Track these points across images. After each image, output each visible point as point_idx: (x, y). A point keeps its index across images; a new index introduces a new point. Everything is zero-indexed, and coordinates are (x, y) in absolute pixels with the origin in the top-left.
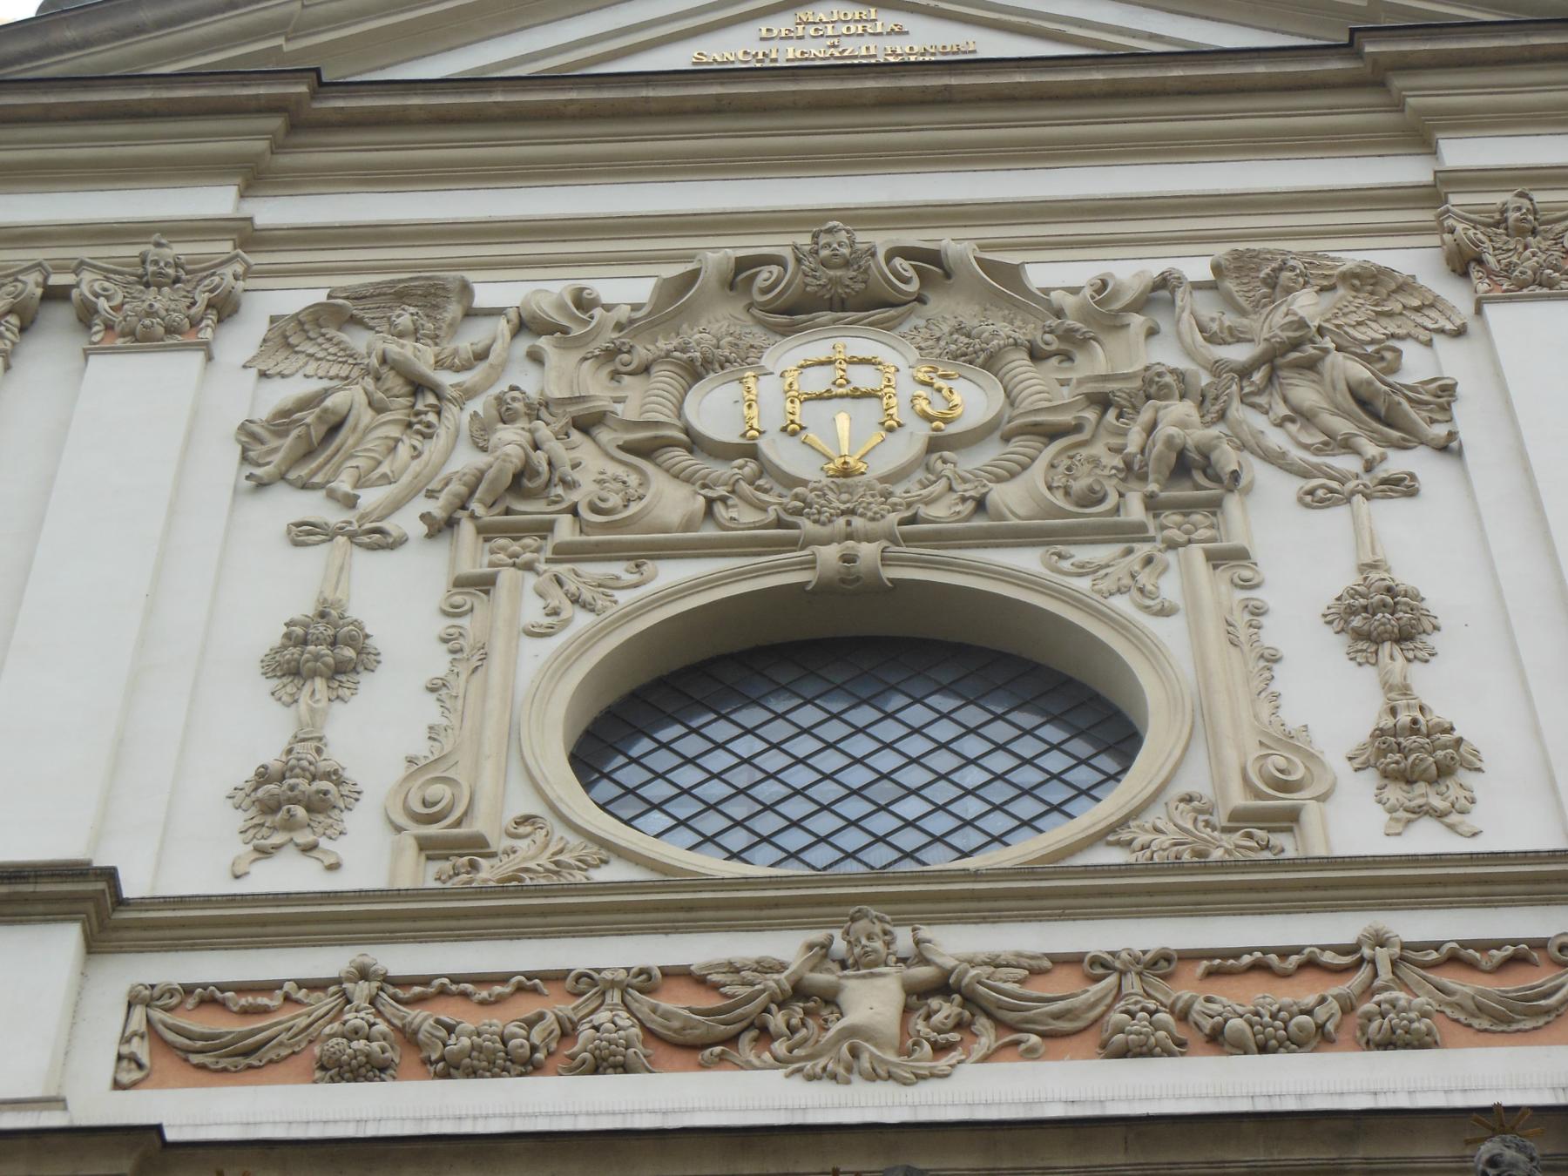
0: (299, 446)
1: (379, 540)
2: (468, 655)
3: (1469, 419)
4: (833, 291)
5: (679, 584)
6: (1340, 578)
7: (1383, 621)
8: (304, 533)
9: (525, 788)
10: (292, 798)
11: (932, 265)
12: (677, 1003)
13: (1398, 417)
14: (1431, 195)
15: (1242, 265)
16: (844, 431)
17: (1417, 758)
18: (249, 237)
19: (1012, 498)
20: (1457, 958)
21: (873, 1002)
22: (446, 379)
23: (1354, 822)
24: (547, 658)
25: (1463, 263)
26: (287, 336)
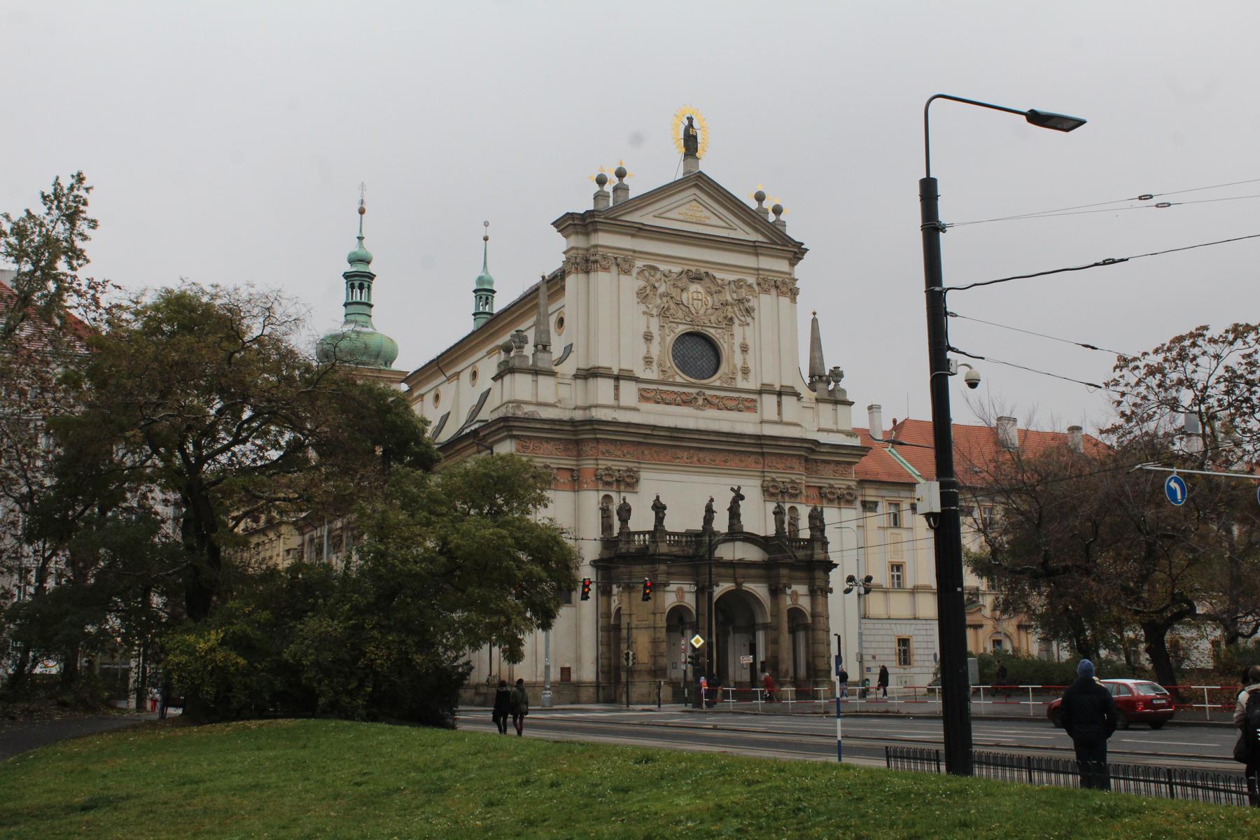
0: (643, 296)
1: (652, 316)
2: (663, 339)
3: (756, 314)
4: (697, 278)
5: (682, 329)
6: (741, 340)
7: (744, 349)
8: (645, 313)
9: (669, 362)
10: (648, 361)
11: (707, 273)
12: (684, 397)
13: (748, 311)
14: (758, 269)
15: (739, 280)
16: (698, 304)
17: (745, 371)
18: (635, 251)
19: (713, 318)
20: (746, 400)
21: (700, 401)
22: (657, 285)
23: (741, 383)
24: (670, 340)
25: (759, 284)
26: (641, 272)
